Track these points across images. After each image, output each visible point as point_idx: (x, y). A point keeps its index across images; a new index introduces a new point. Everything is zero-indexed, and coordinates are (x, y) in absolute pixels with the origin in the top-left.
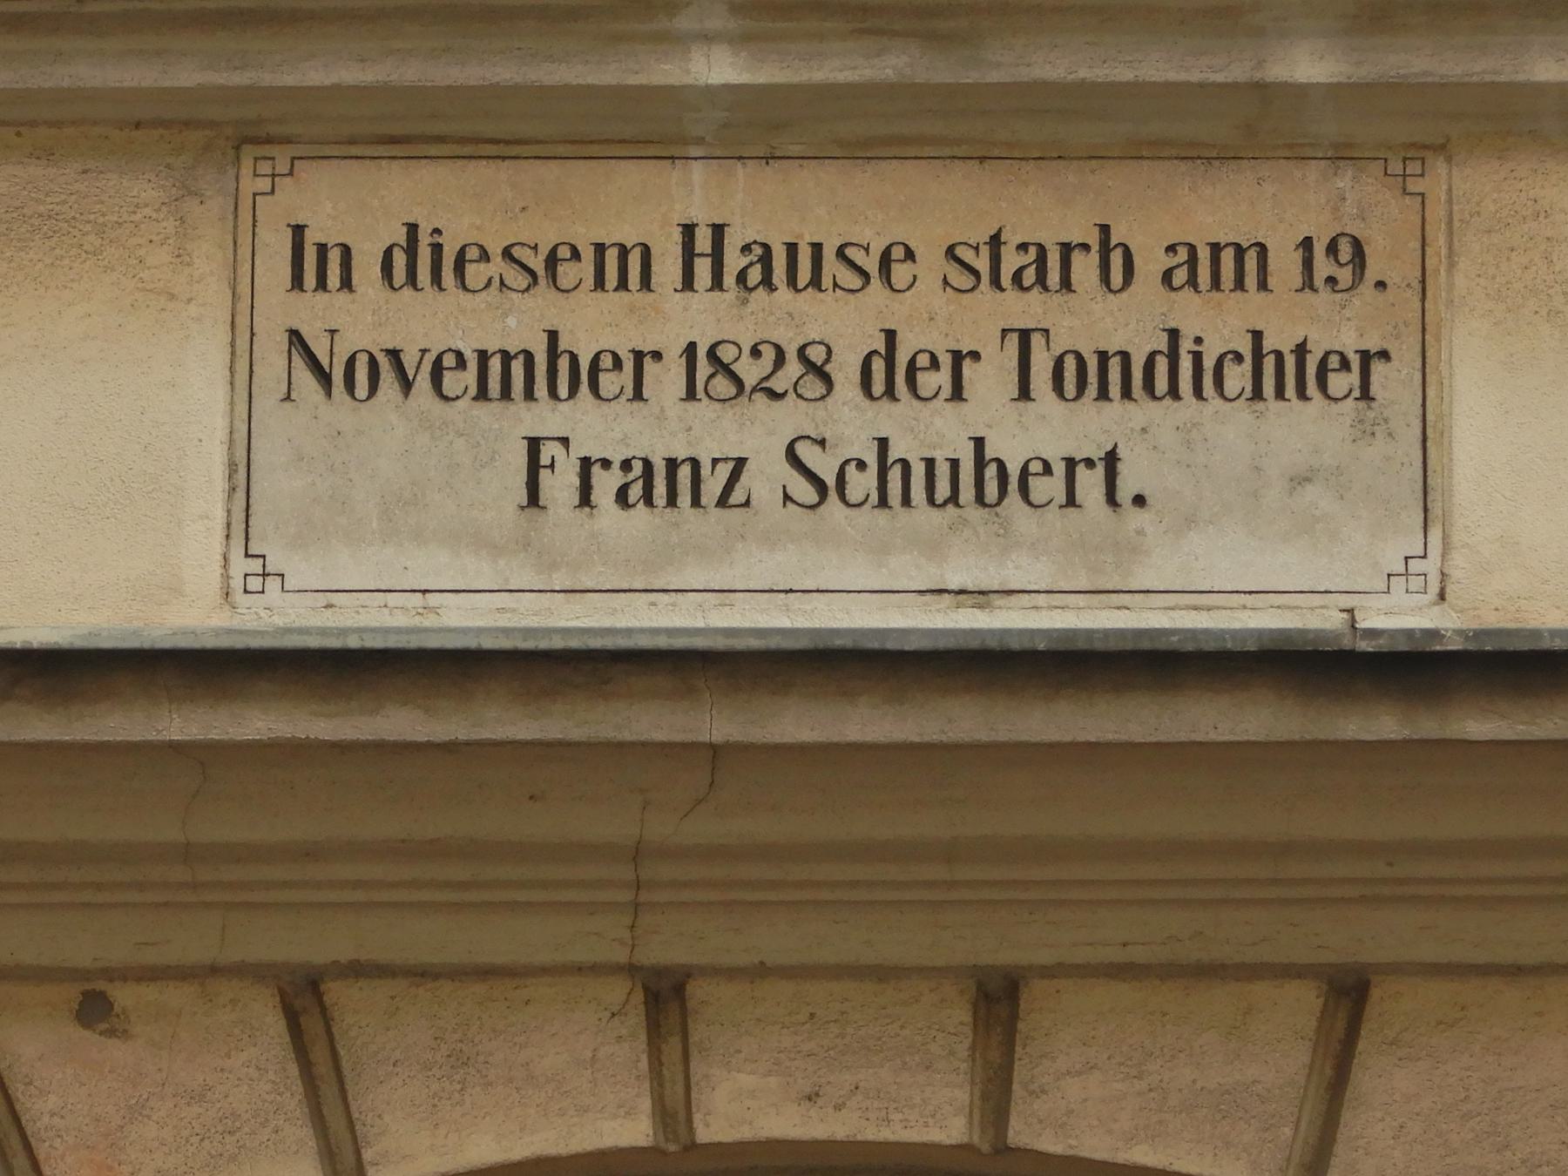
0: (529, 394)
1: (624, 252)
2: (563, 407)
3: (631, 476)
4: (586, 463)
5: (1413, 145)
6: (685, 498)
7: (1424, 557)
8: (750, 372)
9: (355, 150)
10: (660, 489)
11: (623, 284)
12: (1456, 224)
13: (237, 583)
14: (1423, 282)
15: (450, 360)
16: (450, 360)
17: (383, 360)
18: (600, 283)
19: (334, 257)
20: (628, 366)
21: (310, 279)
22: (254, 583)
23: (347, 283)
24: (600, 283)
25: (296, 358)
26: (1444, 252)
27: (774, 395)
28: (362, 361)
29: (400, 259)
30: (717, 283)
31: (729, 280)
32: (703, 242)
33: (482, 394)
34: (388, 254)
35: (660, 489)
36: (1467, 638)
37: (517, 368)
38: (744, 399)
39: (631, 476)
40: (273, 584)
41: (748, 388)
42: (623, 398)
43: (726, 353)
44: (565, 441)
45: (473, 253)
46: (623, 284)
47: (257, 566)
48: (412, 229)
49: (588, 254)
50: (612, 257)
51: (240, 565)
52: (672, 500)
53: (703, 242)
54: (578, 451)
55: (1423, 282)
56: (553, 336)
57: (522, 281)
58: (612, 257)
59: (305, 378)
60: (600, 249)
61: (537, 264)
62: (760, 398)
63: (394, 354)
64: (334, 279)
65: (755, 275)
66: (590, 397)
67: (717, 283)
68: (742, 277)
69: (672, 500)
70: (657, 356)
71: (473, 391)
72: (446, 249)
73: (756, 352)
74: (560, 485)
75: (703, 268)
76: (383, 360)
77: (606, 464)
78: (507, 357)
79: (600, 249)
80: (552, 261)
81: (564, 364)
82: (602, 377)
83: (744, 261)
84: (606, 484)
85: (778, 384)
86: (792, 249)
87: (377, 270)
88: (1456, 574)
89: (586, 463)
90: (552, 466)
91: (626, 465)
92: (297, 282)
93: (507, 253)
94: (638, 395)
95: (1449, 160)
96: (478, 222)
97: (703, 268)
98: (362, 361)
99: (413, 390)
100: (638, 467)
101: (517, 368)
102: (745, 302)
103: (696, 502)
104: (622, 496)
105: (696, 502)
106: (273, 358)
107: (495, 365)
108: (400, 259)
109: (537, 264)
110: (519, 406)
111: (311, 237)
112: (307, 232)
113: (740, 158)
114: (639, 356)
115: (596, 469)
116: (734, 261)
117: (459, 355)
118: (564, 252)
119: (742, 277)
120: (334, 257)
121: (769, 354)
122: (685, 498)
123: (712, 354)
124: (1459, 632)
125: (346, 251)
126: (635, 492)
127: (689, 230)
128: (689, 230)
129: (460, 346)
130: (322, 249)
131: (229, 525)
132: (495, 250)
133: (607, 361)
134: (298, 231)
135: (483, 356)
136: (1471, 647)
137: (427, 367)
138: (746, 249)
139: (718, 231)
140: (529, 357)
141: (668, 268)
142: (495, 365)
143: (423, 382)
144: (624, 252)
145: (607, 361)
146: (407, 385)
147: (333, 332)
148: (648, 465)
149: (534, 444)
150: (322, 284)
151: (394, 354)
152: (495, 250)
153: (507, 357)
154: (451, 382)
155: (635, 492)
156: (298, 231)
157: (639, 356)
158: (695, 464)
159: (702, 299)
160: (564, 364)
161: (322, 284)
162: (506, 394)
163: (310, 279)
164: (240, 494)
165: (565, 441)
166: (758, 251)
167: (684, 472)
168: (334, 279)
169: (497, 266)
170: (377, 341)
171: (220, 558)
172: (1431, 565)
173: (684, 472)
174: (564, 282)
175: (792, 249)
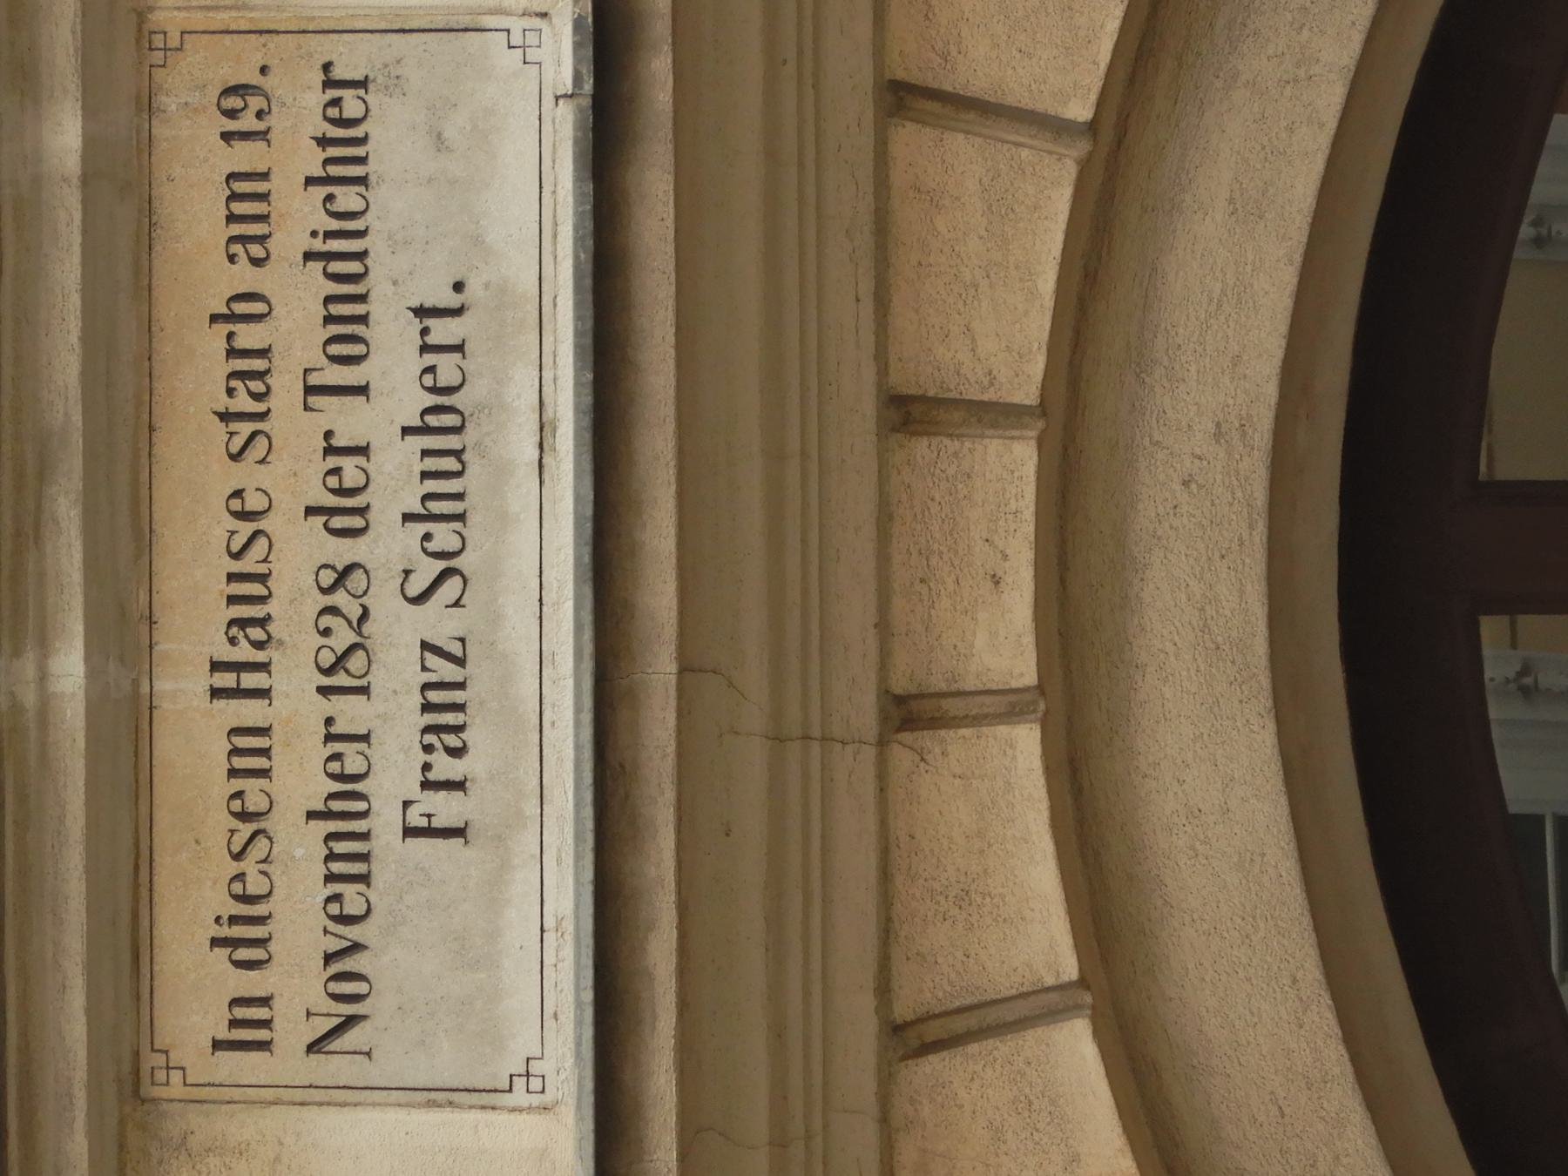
0: (364, 836)
1: (236, 751)
3: (438, 745)
4: (426, 785)
5: (138, 41)
6: (457, 696)
8: (343, 637)
9: (146, 996)
10: (449, 718)
11: (265, 752)
13: (536, 1100)
14: (261, 32)
15: (334, 909)
16: (334, 909)
19: (241, 1013)
20: (338, 747)
21: (261, 1034)
22: (536, 1084)
23: (265, 1001)
24: (264, 773)
25: (331, 1047)
26: (234, 14)
27: (365, 615)
29: (243, 954)
30: (263, 667)
31: (260, 656)
32: (227, 680)
33: (364, 879)
35: (449, 718)
37: (341, 847)
38: (368, 643)
39: (438, 745)
40: (536, 1067)
41: (358, 639)
42: (367, 752)
43: (327, 659)
44: (406, 804)
45: (237, 888)
46: (265, 752)
47: (520, 1083)
48: (215, 942)
49: (238, 784)
50: (241, 763)
51: (519, 1097)
52: (459, 707)
53: (227, 680)
54: (414, 791)
55: (261, 32)
57: (262, 844)
58: (241, 763)
60: (233, 773)
61: (246, 830)
62: (366, 629)
63: (329, 958)
65: (256, 633)
67: (263, 667)
68: (259, 645)
69: (459, 707)
70: (329, 721)
71: (361, 887)
72: (233, 912)
74: (446, 808)
75: (250, 680)
77: (426, 767)
79: (233, 773)
80: (244, 816)
81: (337, 806)
82: (349, 770)
83: (244, 643)
84: (445, 767)
85: (354, 612)
86: (233, 600)
89: (426, 785)
90: (429, 816)
91: (428, 749)
92: (264, 1046)
94: (365, 738)
95: (151, 9)
96: (209, 883)
97: (250, 680)
99: (361, 940)
100: (430, 738)
101: (341, 847)
102: (281, 643)
103: (461, 686)
104: (456, 752)
105: (461, 686)
107: (337, 867)
108: (243, 954)
109: (246, 830)
111: (224, 1033)
112: (219, 1037)
113: (151, 647)
114: (330, 738)
115: (431, 776)
116: (244, 653)
117: (329, 900)
118: (236, 805)
119: (259, 645)
120: (241, 1013)
121: (327, 621)
122: (457, 696)
123: (328, 672)
125: (236, 1002)
126: (452, 740)
127: (216, 693)
128: (216, 693)
129: (321, 899)
130: (234, 1023)
131: (483, 1107)
132: (234, 868)
133: (335, 767)
134: (217, 1045)
135: (330, 878)
138: (233, 641)
139: (216, 666)
140: (331, 837)
141: (250, 712)
142: (337, 867)
143: (353, 932)
145: (335, 767)
146: (356, 947)
147: (309, 1014)
148: (427, 729)
149: (409, 832)
150: (266, 1024)
151: (329, 958)
152: (234, 868)
153: (331, 857)
154: (354, 907)
155: (452, 740)
156: (217, 1045)
157: (330, 738)
158: (426, 687)
159: (278, 681)
160: (337, 806)
161: (266, 1024)
162: (364, 857)
163: (261, 1034)
164: (455, 1097)
165: (406, 804)
166: (234, 631)
167: (435, 696)
169: (249, 866)
171: (512, 1116)
172: (516, 25)
173: (435, 696)
174: (264, 806)
175: (233, 600)
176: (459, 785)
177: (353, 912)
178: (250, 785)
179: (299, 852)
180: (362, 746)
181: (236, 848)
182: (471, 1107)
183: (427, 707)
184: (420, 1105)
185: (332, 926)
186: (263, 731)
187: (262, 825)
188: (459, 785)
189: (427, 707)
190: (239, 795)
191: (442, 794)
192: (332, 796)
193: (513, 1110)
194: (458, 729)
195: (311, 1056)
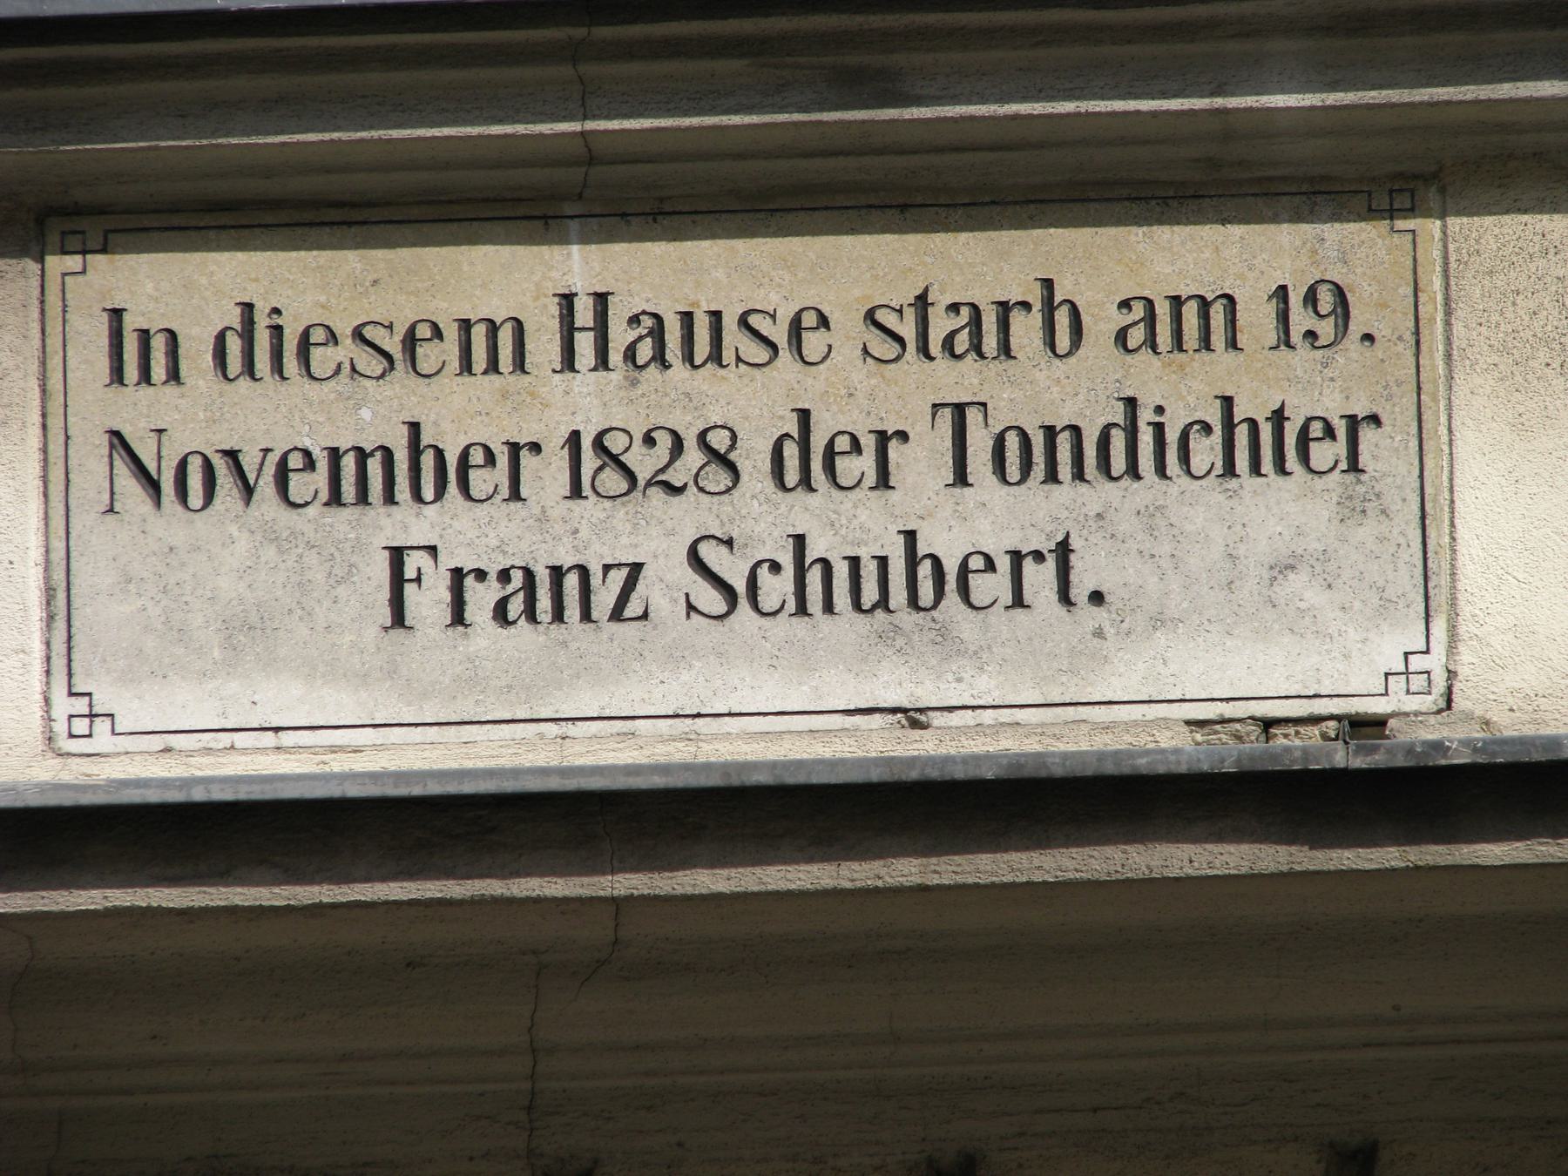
0: (390, 498)
1: (493, 328)
2: (430, 511)
3: (510, 589)
4: (458, 574)
5: (1400, 175)
6: (572, 610)
7: (1427, 652)
8: (644, 463)
9: (176, 220)
10: (544, 603)
11: (493, 366)
12: (1453, 265)
13: (60, 727)
14: (1417, 333)
15: (295, 461)
16: (295, 461)
17: (220, 464)
18: (467, 366)
19: (159, 345)
20: (503, 460)
21: (131, 371)
22: (81, 726)
23: (174, 375)
24: (467, 366)
25: (118, 462)
26: (1440, 298)
27: (674, 490)
28: (195, 465)
29: (234, 345)
30: (602, 362)
31: (615, 357)
32: (584, 314)
33: (335, 499)
34: (221, 339)
35: (544, 603)
36: (1475, 750)
37: (374, 467)
38: (637, 494)
39: (510, 589)
40: (102, 726)
41: (641, 483)
42: (498, 499)
43: (615, 443)
44: (432, 550)
45: (318, 335)
46: (493, 366)
47: (81, 706)
48: (248, 308)
49: (451, 333)
50: (479, 334)
51: (63, 706)
52: (558, 615)
53: (584, 314)
54: (448, 561)
55: (1417, 333)
56: (415, 428)
57: (376, 365)
58: (479, 334)
59: (127, 482)
60: (466, 325)
61: (393, 345)
62: (656, 493)
63: (232, 455)
64: (159, 371)
65: (645, 351)
66: (460, 499)
67: (602, 362)
68: (630, 354)
69: (558, 615)
70: (536, 448)
71: (324, 495)
72: (287, 331)
73: (649, 440)
74: (427, 601)
75: (585, 344)
76: (220, 464)
77: (481, 575)
78: (362, 455)
79: (466, 325)
80: (411, 341)
81: (428, 460)
82: (473, 475)
83: (632, 335)
84: (481, 598)
85: (676, 477)
86: (687, 318)
87: (208, 358)
88: (1463, 671)
89: (458, 574)
90: (418, 580)
91: (504, 576)
92: (117, 375)
93: (358, 335)
94: (515, 495)
95: (1442, 191)
96: (323, 299)
97: (585, 344)
98: (195, 465)
99: (256, 497)
100: (517, 578)
101: (374, 467)
102: (634, 383)
103: (586, 616)
104: (500, 612)
105: (586, 616)
106: (91, 461)
107: (349, 464)
108: (234, 345)
109: (393, 345)
110: (377, 511)
111: (131, 323)
112: (127, 318)
113: (624, 215)
114: (514, 449)
115: (469, 581)
116: (620, 336)
117: (307, 454)
118: (424, 331)
119: (630, 354)
120: (159, 345)
121: (664, 440)
122: (572, 610)
123: (599, 444)
124: (1466, 743)
125: (172, 336)
126: (516, 607)
127: (568, 300)
128: (568, 300)
129: (307, 443)
130: (145, 336)
131: (48, 659)
132: (344, 329)
133: (477, 457)
134: (117, 314)
135: (335, 455)
136: (1481, 759)
137: (270, 469)
138: (634, 320)
139: (602, 300)
140: (387, 453)
141: (544, 346)
142: (349, 464)
143: (266, 487)
144: (493, 328)
145: (477, 457)
146: (248, 491)
147: (160, 431)
148: (529, 574)
149: (397, 555)
150: (145, 376)
151: (232, 455)
152: (344, 329)
153: (362, 455)
154: (300, 486)
155: (516, 607)
156: (117, 314)
157: (514, 449)
158: (583, 571)
159: (585, 380)
160: (428, 460)
161: (145, 376)
162: (363, 498)
163: (131, 371)
164: (60, 624)
165: (432, 550)
166: (648, 322)
167: (572, 582)
168: (159, 371)
169: (347, 349)
170: (211, 441)
171: (39, 698)
172: (1435, 662)
173: (572, 582)
174: (425, 366)
175: (687, 318)
176: (458, 617)
177: (292, 484)
178: (450, 348)
179: (366, 414)
180: (505, 491)
181: (368, 332)
182: (48, 644)
183: (557, 573)
184: (47, 578)
185: (273, 458)
186: (520, 364)
187: (399, 365)
188: (458, 617)
189: (557, 573)
190: (438, 333)
191: (447, 596)
192: (439, 454)
193: (47, 700)
194: (531, 613)
195: (107, 436)
